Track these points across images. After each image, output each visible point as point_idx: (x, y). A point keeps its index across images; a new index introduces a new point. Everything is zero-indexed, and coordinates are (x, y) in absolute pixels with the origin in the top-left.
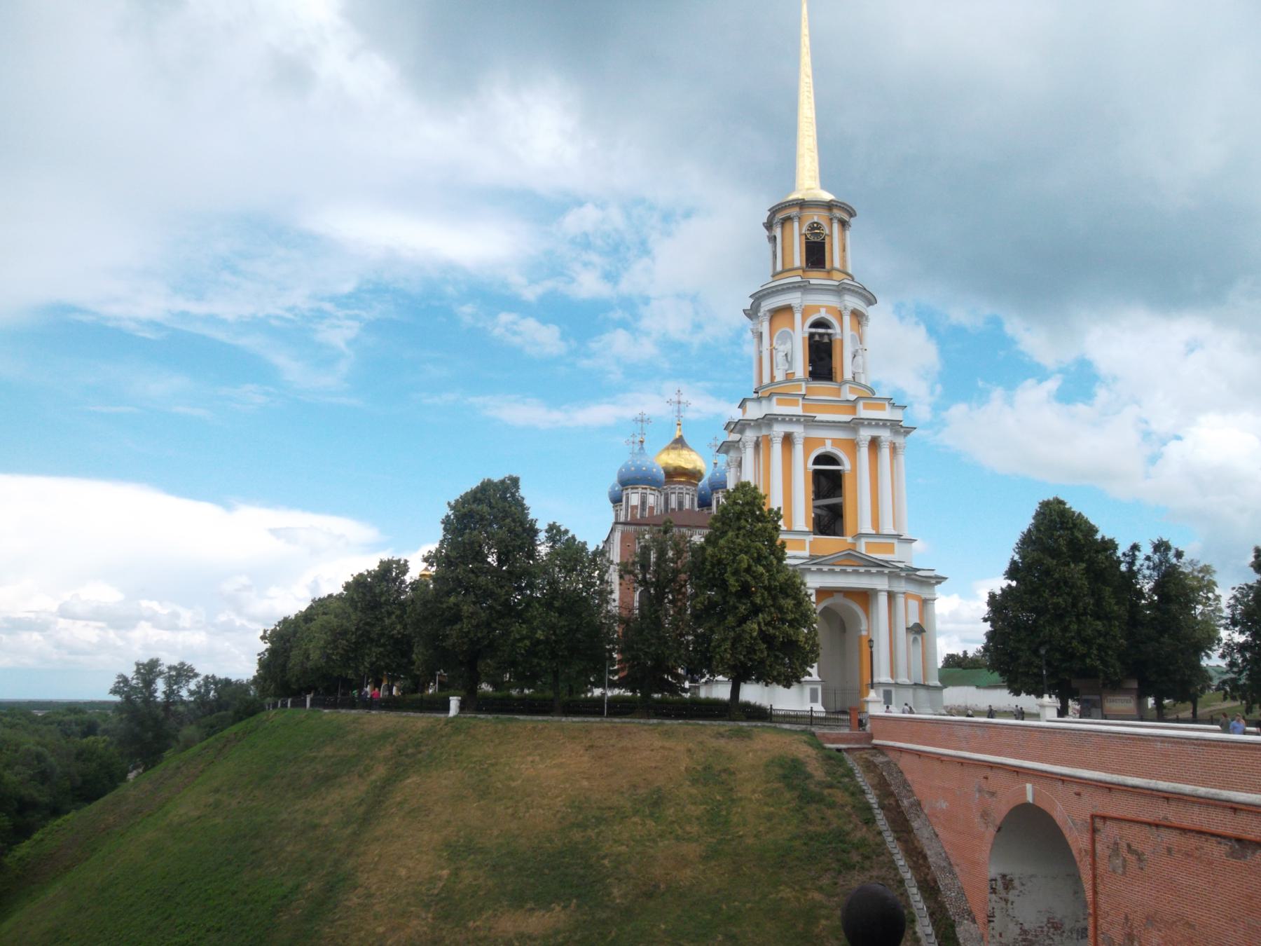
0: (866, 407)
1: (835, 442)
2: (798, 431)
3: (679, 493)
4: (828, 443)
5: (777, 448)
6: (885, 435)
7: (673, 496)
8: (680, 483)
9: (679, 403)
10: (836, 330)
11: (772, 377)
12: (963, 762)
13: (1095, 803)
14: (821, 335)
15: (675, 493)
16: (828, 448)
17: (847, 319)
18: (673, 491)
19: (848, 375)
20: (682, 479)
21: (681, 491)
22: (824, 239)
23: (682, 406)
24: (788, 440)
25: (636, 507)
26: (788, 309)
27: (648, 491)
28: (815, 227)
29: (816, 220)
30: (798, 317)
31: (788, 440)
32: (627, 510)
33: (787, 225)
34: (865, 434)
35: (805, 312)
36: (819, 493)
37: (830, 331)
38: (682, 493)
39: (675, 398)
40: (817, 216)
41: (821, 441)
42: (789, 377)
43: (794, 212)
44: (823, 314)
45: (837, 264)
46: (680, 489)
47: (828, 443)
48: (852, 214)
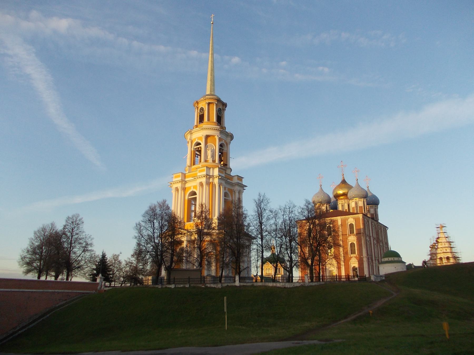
0: (200, 171)
3: (342, 203)
4: (192, 187)
8: (342, 199)
14: (198, 148)
15: (340, 204)
17: (204, 140)
18: (345, 202)
20: (342, 198)
21: (342, 202)
22: (204, 112)
34: (199, 181)
37: (200, 146)
38: (343, 203)
41: (190, 188)
44: (197, 141)
46: (342, 201)
47: (192, 187)
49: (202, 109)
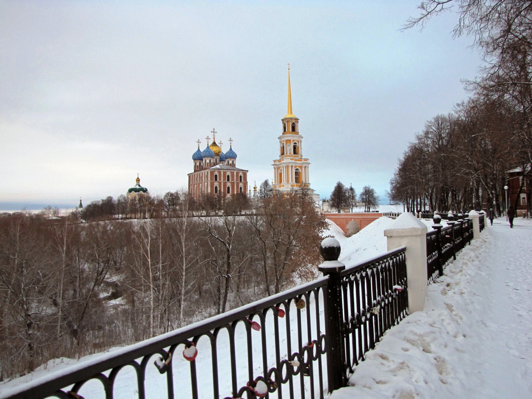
1: (299, 166)
2: (294, 165)
5: (290, 168)
6: (307, 165)
7: (214, 159)
9: (214, 132)
10: (297, 145)
11: (287, 153)
12: (342, 218)
13: (360, 220)
16: (298, 168)
19: (300, 153)
23: (215, 133)
24: (292, 167)
25: (208, 163)
26: (290, 140)
27: (211, 159)
28: (293, 124)
29: (294, 122)
30: (292, 142)
31: (292, 167)
32: (205, 164)
33: (288, 122)
35: (294, 141)
36: (296, 175)
39: (213, 131)
40: (294, 121)
42: (290, 153)
43: (290, 120)
44: (296, 142)
45: (297, 131)
48: (299, 120)
49: (293, 124)
